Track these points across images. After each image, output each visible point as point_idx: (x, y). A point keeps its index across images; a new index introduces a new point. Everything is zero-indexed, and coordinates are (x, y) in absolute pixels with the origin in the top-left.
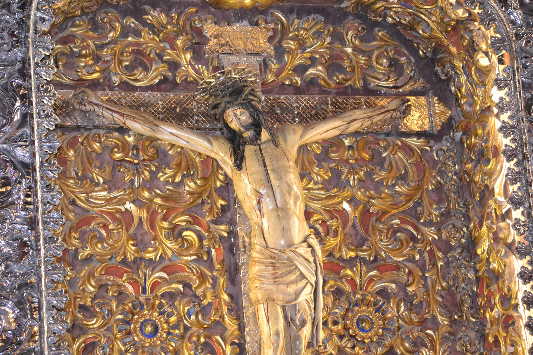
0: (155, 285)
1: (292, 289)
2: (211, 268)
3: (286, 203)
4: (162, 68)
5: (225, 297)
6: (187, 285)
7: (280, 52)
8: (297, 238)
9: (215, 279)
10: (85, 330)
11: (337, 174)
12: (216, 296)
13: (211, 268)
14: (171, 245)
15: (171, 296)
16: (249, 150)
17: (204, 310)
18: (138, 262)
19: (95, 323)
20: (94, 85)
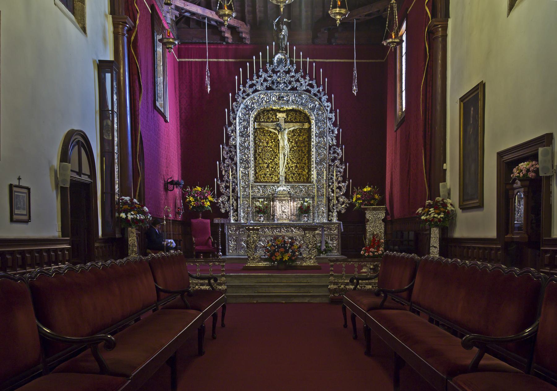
0: (269, 149)
1: (284, 151)
2: (276, 147)
3: (284, 140)
4: (272, 119)
5: (278, 151)
6: (273, 149)
7: (288, 117)
8: (286, 144)
9: (277, 149)
10: (260, 155)
11: (294, 134)
12: (277, 151)
13: (276, 147)
14: (271, 144)
15: (271, 151)
16: (280, 132)
17: (275, 153)
18: (266, 147)
19: (261, 154)
20: (262, 122)
